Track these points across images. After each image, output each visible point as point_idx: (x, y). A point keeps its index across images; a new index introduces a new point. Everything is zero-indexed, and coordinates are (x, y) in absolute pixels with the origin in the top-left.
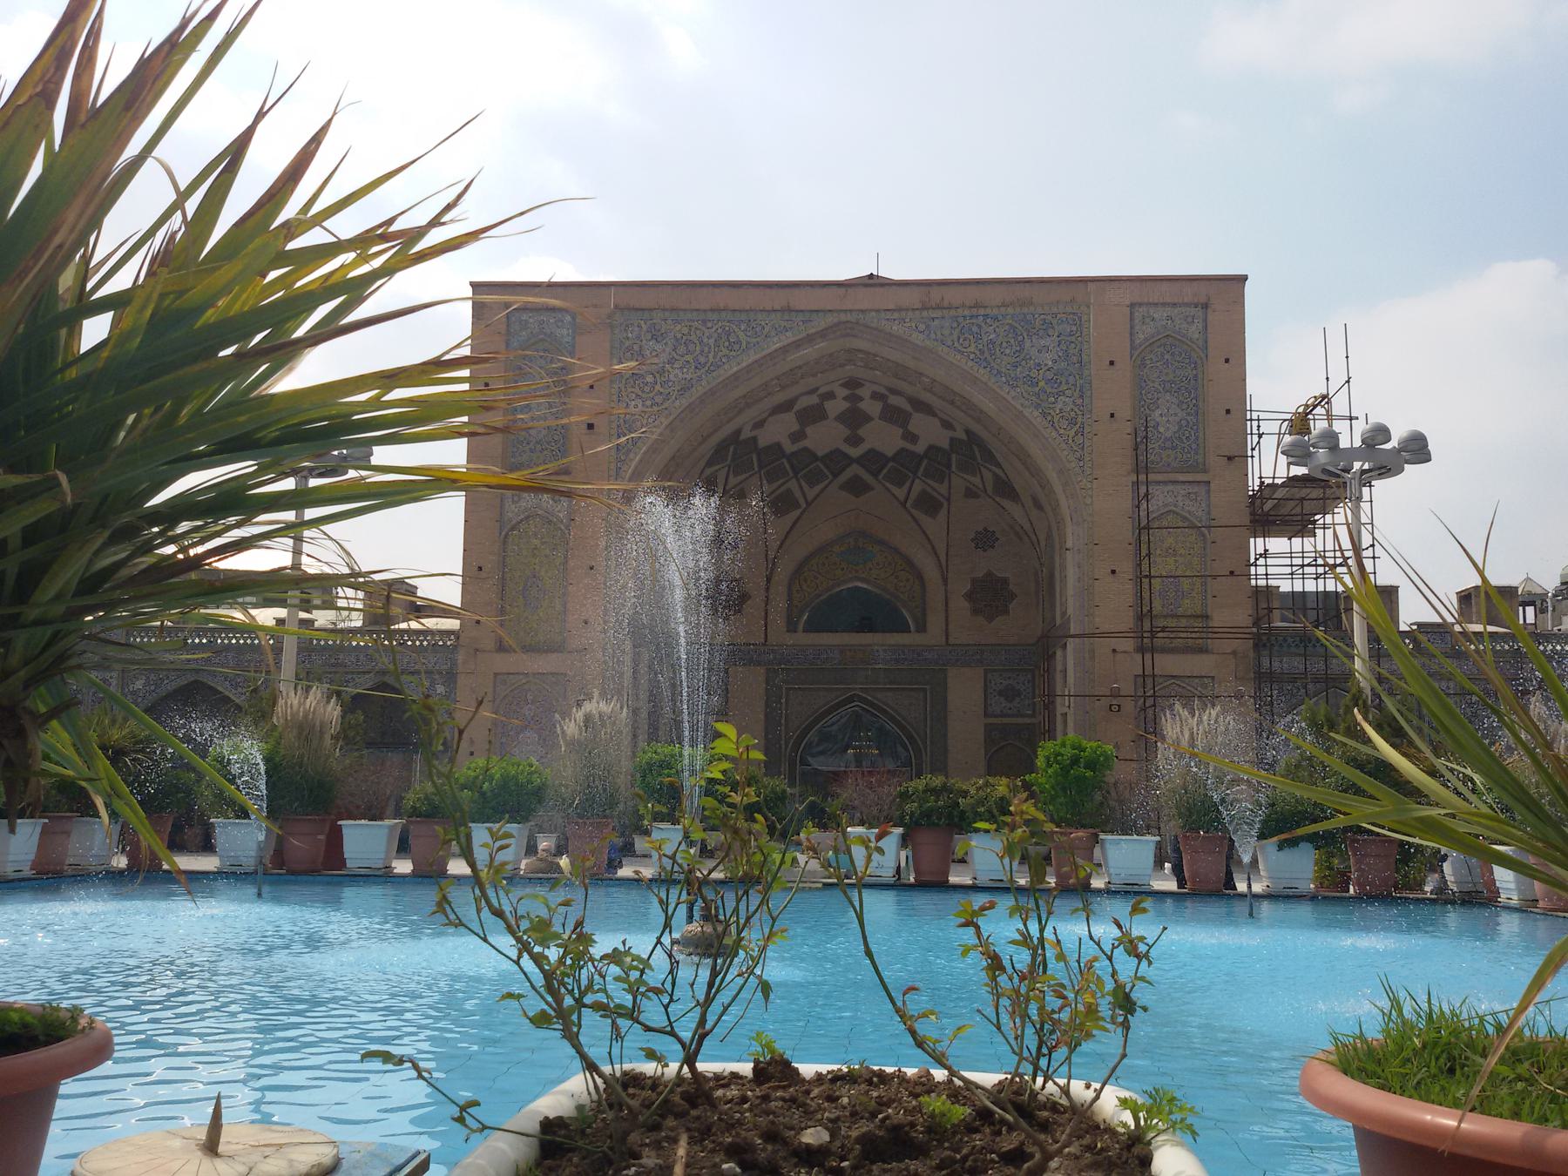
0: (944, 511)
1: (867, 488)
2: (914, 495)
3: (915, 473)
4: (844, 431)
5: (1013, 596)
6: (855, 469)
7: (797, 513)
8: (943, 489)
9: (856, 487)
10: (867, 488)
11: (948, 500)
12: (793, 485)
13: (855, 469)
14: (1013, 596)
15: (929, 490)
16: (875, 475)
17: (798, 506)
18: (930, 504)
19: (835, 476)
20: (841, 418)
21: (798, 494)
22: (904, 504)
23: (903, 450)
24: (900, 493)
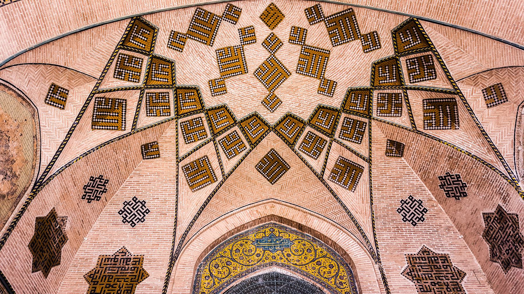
0: (365, 175)
1: (284, 167)
2: (331, 164)
3: (331, 135)
4: (260, 90)
5: (461, 275)
6: (272, 142)
7: (211, 188)
8: (362, 149)
9: (273, 168)
10: (284, 167)
11: (369, 161)
12: (209, 150)
13: (272, 142)
14: (461, 275)
15: (348, 155)
16: (291, 145)
17: (212, 178)
18: (348, 172)
19: (254, 145)
20: (259, 73)
21: (215, 164)
22: (320, 178)
23: (321, 107)
24: (317, 164)
